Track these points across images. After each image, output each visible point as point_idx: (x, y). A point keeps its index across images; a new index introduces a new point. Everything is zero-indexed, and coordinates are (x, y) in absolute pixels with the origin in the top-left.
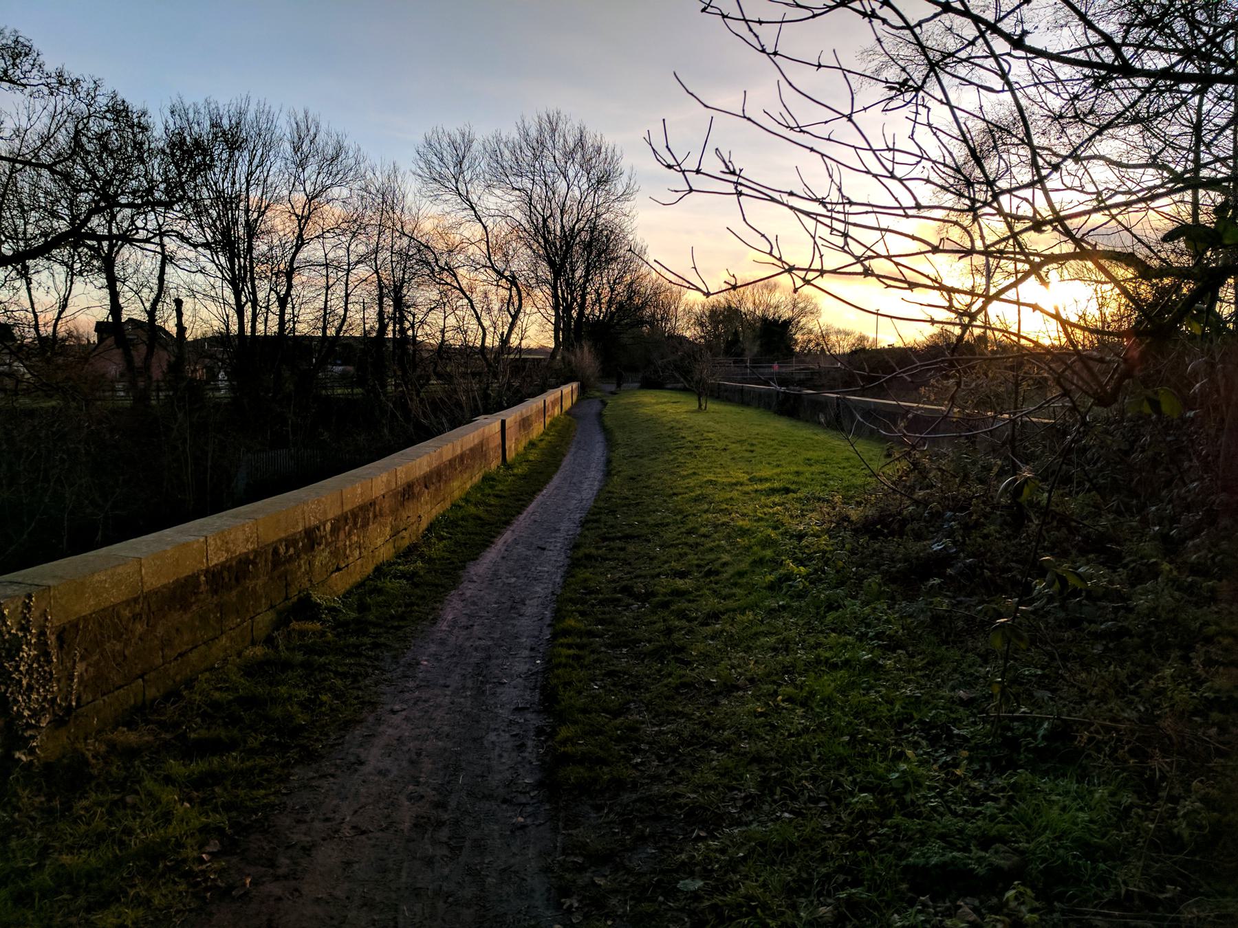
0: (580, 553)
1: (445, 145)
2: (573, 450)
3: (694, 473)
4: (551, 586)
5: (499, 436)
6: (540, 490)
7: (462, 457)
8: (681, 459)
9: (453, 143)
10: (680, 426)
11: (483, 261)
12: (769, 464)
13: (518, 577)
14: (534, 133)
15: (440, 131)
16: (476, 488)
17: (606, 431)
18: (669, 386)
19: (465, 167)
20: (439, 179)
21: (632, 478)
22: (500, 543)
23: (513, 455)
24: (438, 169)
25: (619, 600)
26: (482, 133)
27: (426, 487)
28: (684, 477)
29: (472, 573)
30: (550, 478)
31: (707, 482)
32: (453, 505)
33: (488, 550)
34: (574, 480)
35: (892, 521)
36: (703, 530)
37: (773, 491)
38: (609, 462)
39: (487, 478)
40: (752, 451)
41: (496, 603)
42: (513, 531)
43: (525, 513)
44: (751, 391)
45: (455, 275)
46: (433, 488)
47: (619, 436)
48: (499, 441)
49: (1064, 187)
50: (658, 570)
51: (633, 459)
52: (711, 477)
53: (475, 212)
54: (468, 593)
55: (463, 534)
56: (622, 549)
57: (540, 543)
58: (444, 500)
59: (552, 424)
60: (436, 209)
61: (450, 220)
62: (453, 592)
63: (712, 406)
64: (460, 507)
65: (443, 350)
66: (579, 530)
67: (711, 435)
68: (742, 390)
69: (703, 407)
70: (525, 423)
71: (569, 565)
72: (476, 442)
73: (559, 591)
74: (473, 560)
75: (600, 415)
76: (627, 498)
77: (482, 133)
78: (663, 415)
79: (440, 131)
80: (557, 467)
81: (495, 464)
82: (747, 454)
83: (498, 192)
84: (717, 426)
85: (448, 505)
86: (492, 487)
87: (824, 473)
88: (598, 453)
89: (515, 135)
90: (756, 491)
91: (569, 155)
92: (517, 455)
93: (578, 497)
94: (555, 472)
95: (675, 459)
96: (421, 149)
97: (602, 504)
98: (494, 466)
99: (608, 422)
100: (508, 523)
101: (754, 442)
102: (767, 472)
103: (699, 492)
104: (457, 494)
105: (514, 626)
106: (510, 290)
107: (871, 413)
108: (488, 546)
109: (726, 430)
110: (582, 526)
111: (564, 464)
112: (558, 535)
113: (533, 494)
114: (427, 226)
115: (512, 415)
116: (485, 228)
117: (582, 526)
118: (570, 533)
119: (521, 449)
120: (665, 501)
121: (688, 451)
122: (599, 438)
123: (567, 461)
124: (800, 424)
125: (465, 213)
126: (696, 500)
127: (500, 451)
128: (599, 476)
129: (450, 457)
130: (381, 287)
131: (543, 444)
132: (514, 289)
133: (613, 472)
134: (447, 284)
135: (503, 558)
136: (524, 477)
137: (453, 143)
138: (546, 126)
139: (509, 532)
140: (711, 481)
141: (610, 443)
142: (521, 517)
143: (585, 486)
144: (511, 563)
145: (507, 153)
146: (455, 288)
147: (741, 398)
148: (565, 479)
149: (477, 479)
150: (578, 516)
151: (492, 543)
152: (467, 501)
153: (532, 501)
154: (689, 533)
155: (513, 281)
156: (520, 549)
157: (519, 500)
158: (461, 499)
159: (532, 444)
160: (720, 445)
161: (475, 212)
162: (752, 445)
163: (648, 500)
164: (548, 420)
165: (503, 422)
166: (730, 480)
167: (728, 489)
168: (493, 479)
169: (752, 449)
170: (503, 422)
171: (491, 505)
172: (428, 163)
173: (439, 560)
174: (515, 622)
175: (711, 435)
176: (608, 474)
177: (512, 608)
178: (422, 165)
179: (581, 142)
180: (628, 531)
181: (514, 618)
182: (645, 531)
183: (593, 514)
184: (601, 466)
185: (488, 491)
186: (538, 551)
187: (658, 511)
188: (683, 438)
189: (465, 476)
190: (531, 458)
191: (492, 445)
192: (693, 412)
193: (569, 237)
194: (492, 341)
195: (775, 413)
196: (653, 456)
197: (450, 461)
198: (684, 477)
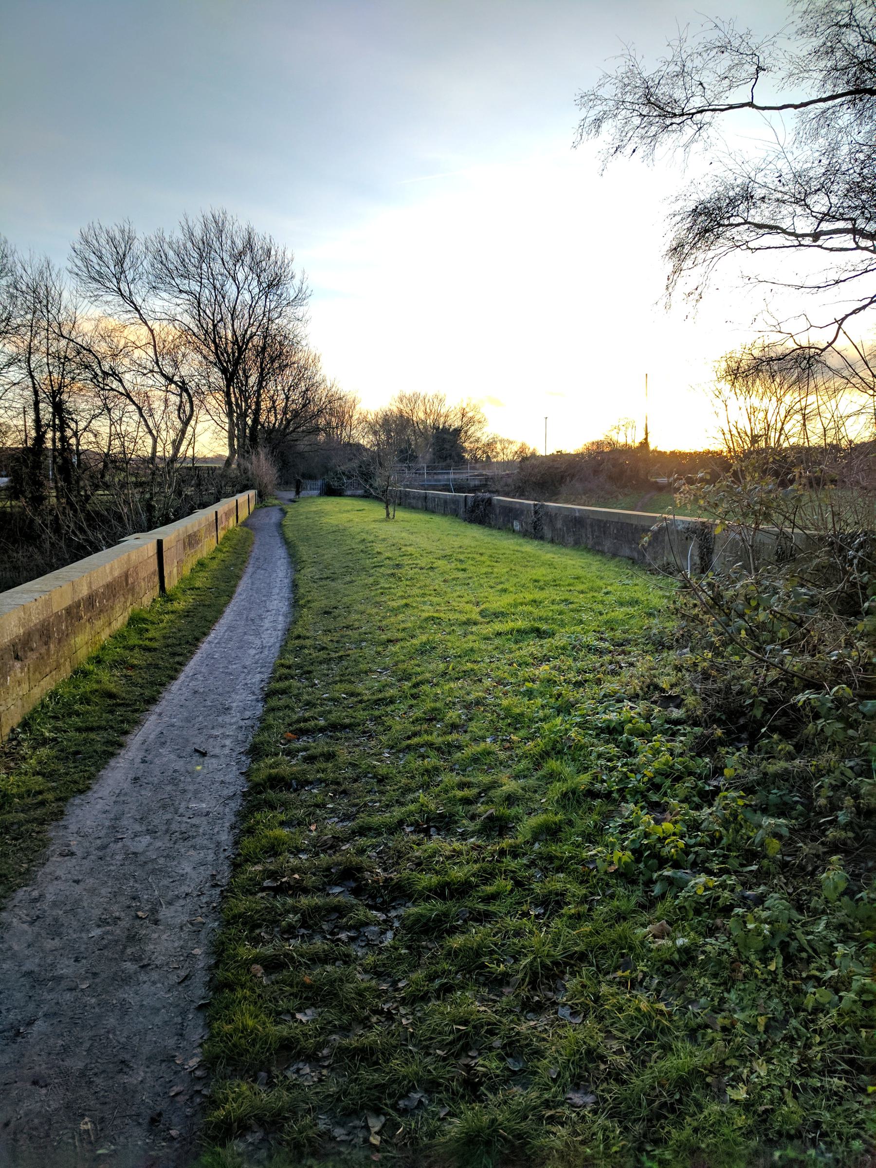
0: (264, 768)
1: (103, 241)
2: (250, 570)
3: (407, 605)
4: (211, 857)
5: (154, 561)
6: (205, 634)
7: (90, 600)
8: (384, 583)
9: (111, 240)
10: (371, 538)
11: (149, 365)
12: (492, 587)
13: (151, 832)
14: (198, 233)
15: (97, 226)
16: (118, 637)
17: (287, 543)
18: (349, 493)
19: (126, 266)
20: (98, 278)
21: (326, 613)
22: (135, 741)
23: (176, 583)
24: (97, 268)
25: (340, 910)
26: (143, 233)
27: (17, 658)
28: (395, 611)
29: (73, 828)
30: (220, 612)
31: (427, 619)
32: (75, 672)
33: (112, 762)
34: (252, 615)
35: (752, 705)
36: (453, 715)
37: (522, 633)
38: (295, 586)
39: (134, 620)
40: (464, 570)
41: (102, 922)
42: (160, 714)
43: (182, 677)
44: (434, 498)
45: (120, 381)
46: (33, 656)
47: (304, 551)
48: (155, 566)
49: (854, 246)
50: (398, 812)
51: (324, 582)
52: (428, 611)
53: (140, 315)
54: (51, 892)
55: (79, 730)
56: (330, 756)
57: (198, 741)
58: (58, 667)
59: (226, 538)
60: (95, 311)
61: (112, 323)
62: (21, 894)
63: (401, 514)
64: (86, 674)
65: (108, 460)
66: (260, 709)
67: (410, 549)
68: (426, 497)
69: (391, 516)
70: (191, 541)
71: (244, 795)
72: (116, 573)
73: (224, 880)
74: (81, 792)
75: (280, 526)
76: (323, 648)
77: (143, 233)
78: (350, 524)
79: (97, 226)
80: (230, 597)
81: (148, 597)
82: (460, 575)
83: (164, 295)
84: (412, 537)
85: (66, 672)
86: (141, 632)
87: (566, 600)
88: (281, 572)
89: (179, 236)
90: (499, 634)
91: (238, 258)
92: (182, 580)
93: (258, 642)
94: (226, 604)
95: (376, 583)
96: (77, 246)
97: (290, 659)
98: (147, 601)
99: (290, 535)
100: (153, 700)
101: (462, 557)
102: (498, 603)
103: (424, 638)
104: (82, 654)
105: (124, 1008)
106: (181, 396)
107: (577, 522)
108: (112, 755)
109: (425, 544)
110: (265, 700)
111: (239, 590)
112: (227, 719)
113: (195, 642)
114: (86, 327)
115: (170, 533)
116: (152, 331)
117: (265, 700)
118: (248, 714)
119: (187, 572)
120: (379, 653)
121: (389, 572)
122: (281, 552)
123: (243, 585)
124: (494, 532)
125: (129, 316)
126: (425, 650)
127: (156, 579)
128: (284, 607)
129: (68, 602)
130: (36, 393)
131: (214, 565)
132: (184, 394)
133: (302, 602)
134: (112, 389)
135: (136, 779)
136: (187, 614)
137: (111, 240)
138: (212, 226)
139: (153, 718)
140: (433, 618)
141: (295, 561)
142: (175, 686)
143: (267, 624)
144: (147, 793)
145: (171, 254)
146: (122, 394)
147: (427, 506)
148: (240, 614)
149: (119, 621)
150: (258, 677)
151: (121, 745)
152: (98, 661)
153: (192, 653)
154: (432, 718)
155: (183, 387)
156: (167, 757)
157: (174, 654)
158: (90, 659)
159: (201, 564)
160: (423, 562)
161: (140, 315)
162: (461, 561)
163: (354, 653)
164: (221, 534)
165: (160, 543)
166: (457, 616)
167: (459, 631)
168: (144, 620)
169: (463, 567)
170: (160, 543)
171: (133, 667)
172: (85, 260)
173: (21, 797)
174: (128, 994)
175: (409, 548)
176: (296, 603)
177: (132, 938)
178: (79, 263)
179: (249, 245)
180: (338, 715)
181: (126, 980)
182: (361, 715)
183: (280, 679)
184: (286, 593)
185: (134, 640)
186: (196, 757)
187: (371, 671)
188: (379, 553)
189: (99, 623)
190: (198, 584)
191: (143, 574)
192: (381, 521)
193: (241, 344)
194: (165, 450)
195: (465, 520)
196: (348, 579)
197: (68, 610)
198: (395, 611)
